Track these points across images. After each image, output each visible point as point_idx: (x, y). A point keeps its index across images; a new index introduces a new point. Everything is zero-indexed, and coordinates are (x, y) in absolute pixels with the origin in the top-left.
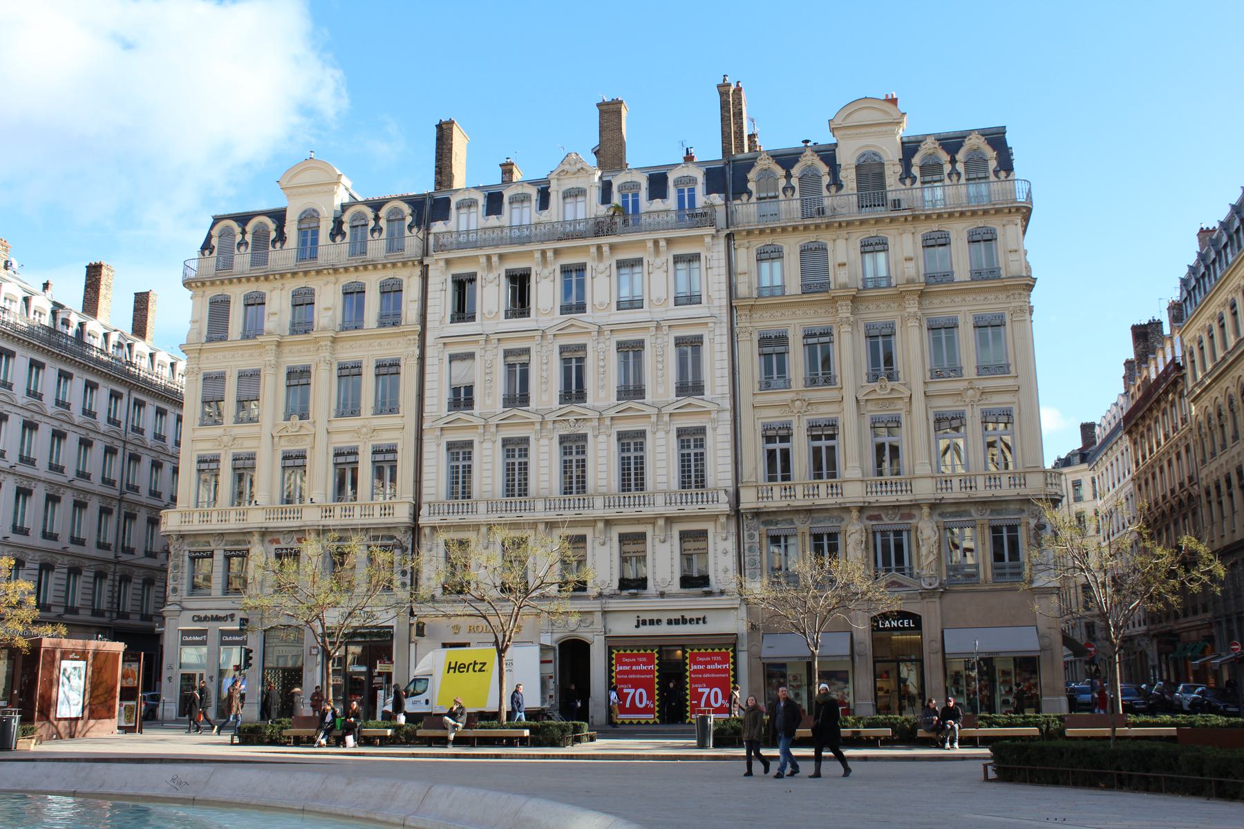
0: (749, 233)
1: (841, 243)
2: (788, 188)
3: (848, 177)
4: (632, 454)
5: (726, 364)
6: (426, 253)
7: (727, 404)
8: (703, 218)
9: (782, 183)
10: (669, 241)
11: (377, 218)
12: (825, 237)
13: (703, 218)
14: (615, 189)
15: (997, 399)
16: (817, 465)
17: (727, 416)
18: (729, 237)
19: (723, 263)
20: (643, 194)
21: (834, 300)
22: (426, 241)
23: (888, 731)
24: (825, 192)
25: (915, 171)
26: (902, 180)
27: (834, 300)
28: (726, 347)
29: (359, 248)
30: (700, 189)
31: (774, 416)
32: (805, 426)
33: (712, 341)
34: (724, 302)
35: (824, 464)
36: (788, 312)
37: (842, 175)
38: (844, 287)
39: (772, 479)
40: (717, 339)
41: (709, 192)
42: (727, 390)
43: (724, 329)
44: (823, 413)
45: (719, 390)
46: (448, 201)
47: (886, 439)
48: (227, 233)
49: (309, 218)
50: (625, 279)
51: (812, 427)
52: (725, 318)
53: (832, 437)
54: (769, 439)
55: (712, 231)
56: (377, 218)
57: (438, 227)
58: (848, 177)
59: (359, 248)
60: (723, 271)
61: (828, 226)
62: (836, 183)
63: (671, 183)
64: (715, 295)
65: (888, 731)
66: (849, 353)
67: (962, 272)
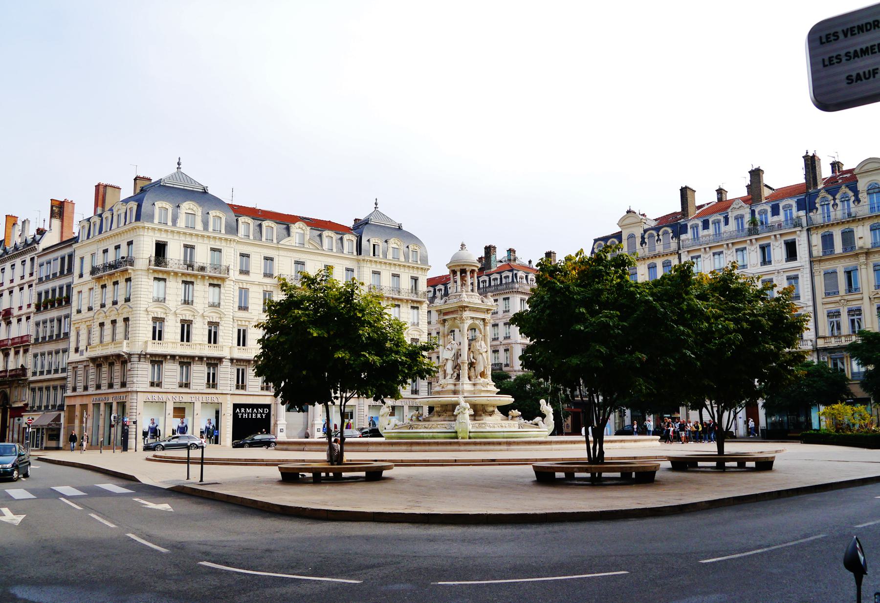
0: (817, 228)
1: (860, 228)
5: (810, 286)
6: (679, 249)
7: (811, 303)
8: (797, 224)
10: (733, 244)
11: (658, 235)
12: (853, 226)
13: (797, 224)
14: (756, 213)
18: (808, 230)
19: (806, 242)
20: (769, 214)
21: (857, 255)
22: (679, 243)
23: (363, 474)
27: (857, 255)
28: (809, 279)
29: (652, 248)
30: (794, 209)
31: (832, 307)
32: (846, 310)
33: (802, 276)
34: (807, 259)
36: (837, 261)
37: (860, 196)
38: (861, 248)
41: (798, 210)
42: (810, 297)
43: (808, 270)
44: (854, 305)
45: (807, 298)
46: (686, 225)
48: (600, 245)
49: (631, 237)
50: (717, 261)
51: (849, 311)
52: (808, 266)
55: (800, 229)
56: (658, 235)
57: (683, 237)
59: (652, 248)
60: (806, 245)
61: (853, 221)
62: (857, 200)
63: (781, 208)
64: (803, 256)
65: (363, 474)
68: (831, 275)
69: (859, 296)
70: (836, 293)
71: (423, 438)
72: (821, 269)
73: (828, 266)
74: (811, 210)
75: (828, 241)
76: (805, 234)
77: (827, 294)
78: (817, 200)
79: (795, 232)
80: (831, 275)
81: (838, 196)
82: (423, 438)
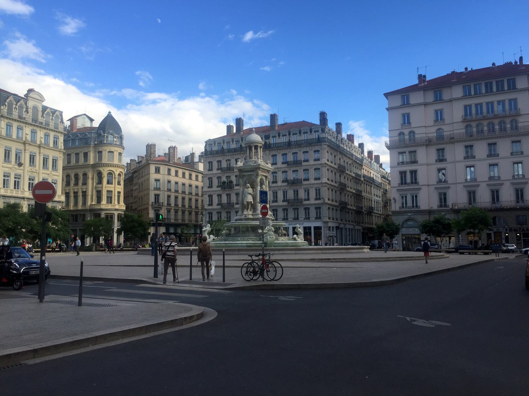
1: (27, 128)
3: (30, 111)
16: (15, 185)
26: (42, 117)
35: (17, 185)
36: (12, 143)
37: (29, 110)
39: (15, 188)
47: (31, 182)
54: (4, 176)
62: (27, 111)
78: (8, 101)
81: (18, 104)
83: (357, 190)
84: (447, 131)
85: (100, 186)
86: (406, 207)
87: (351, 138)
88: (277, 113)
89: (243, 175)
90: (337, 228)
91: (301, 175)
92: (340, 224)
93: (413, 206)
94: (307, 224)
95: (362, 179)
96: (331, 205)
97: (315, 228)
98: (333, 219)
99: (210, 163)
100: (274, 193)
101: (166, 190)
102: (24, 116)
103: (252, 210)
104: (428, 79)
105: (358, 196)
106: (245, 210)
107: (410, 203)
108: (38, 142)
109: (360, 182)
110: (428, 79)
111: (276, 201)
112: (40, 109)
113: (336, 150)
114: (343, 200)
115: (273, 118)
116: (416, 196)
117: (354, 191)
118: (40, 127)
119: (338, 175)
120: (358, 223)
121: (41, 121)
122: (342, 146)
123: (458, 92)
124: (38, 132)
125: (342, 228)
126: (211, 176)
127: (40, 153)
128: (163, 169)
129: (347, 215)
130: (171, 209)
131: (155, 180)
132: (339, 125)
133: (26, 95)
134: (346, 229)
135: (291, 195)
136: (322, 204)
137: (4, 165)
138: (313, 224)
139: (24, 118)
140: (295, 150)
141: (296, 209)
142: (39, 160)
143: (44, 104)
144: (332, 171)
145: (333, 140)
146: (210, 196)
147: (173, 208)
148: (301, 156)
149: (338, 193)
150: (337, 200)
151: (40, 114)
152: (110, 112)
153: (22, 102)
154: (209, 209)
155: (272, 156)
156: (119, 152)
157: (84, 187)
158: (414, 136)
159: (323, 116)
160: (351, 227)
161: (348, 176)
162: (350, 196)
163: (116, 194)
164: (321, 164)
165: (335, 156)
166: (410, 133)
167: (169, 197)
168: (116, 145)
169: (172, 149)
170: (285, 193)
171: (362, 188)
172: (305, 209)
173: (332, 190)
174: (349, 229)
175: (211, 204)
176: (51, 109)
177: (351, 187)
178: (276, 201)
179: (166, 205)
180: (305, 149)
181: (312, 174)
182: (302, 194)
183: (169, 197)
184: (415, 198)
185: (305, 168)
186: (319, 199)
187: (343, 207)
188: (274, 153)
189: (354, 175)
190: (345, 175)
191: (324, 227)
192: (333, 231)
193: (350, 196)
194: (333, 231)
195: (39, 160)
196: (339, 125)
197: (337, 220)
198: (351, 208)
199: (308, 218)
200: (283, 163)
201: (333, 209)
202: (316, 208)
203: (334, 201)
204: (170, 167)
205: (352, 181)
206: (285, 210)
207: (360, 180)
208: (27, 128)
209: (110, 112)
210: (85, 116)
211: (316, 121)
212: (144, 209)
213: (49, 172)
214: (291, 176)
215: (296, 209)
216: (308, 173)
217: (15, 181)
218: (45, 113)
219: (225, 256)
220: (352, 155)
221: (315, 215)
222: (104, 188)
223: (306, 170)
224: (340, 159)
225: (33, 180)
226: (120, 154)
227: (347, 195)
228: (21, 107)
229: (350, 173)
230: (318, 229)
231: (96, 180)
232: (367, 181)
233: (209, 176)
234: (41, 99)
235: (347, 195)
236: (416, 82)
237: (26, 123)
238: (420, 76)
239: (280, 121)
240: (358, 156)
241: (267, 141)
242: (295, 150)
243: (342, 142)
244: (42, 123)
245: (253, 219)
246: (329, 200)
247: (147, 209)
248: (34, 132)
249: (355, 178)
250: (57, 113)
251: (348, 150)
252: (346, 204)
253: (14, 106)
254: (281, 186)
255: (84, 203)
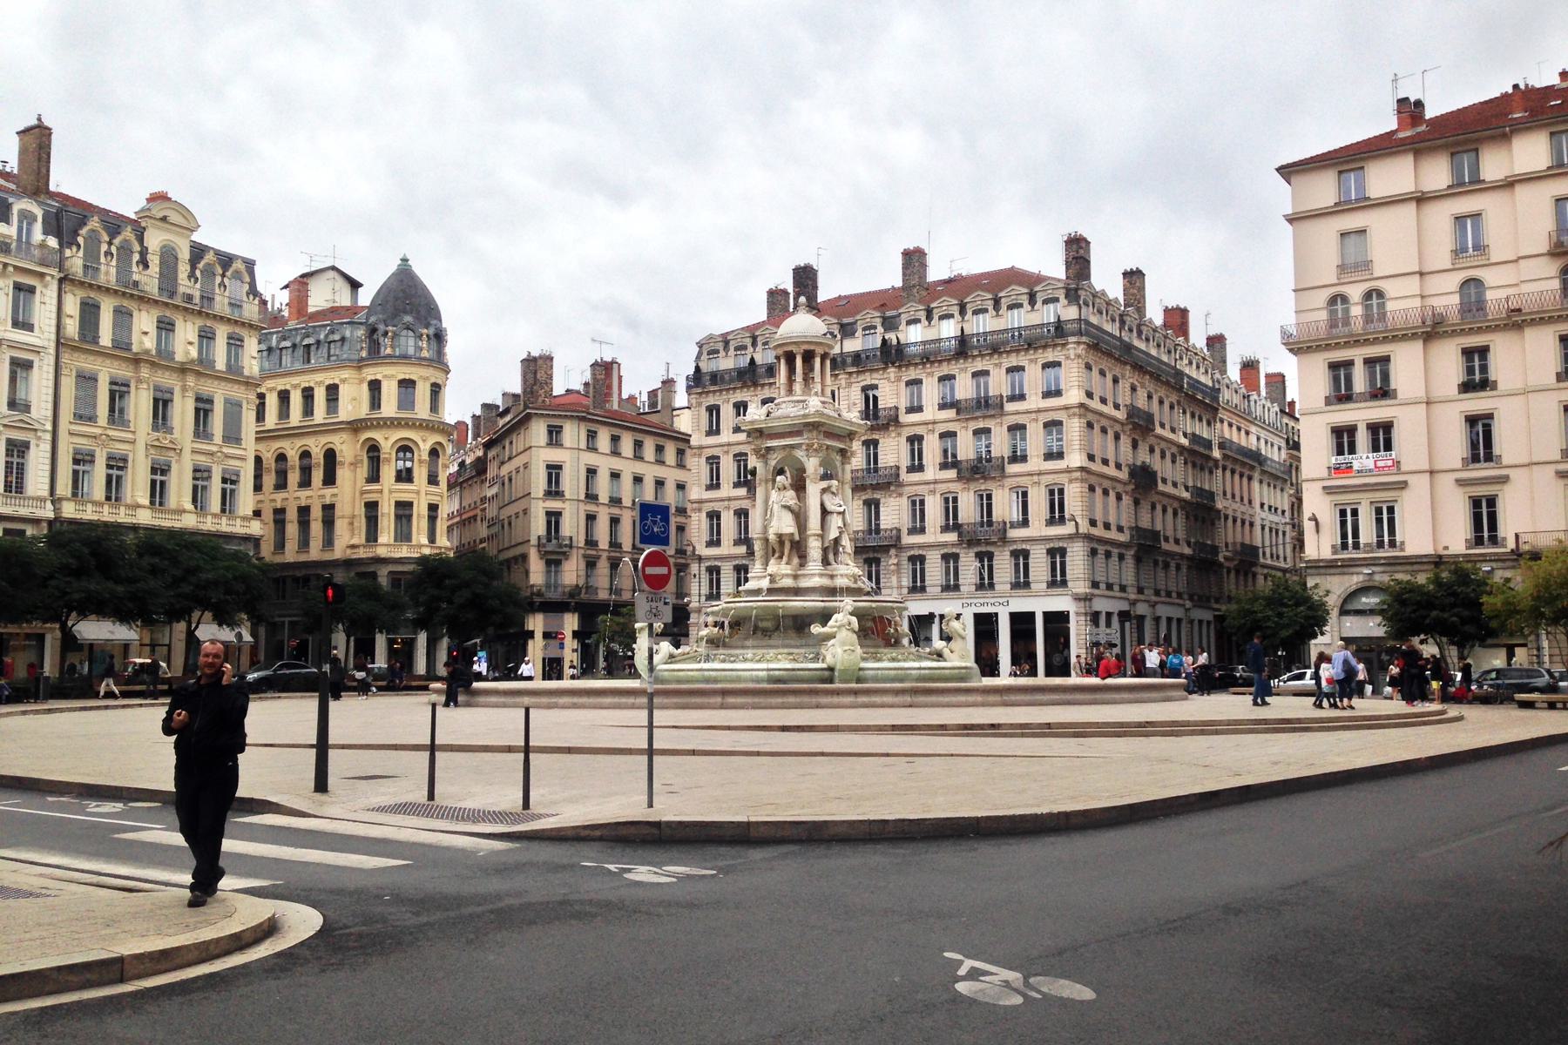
2: (108, 253)
3: (154, 261)
4: (15, 460)
7: (49, 427)
9: (104, 247)
15: (232, 462)
17: (48, 437)
18: (61, 281)
19: (55, 301)
24: (135, 268)
25: (198, 273)
26: (189, 277)
28: (51, 376)
30: (38, 227)
33: (40, 367)
34: (53, 337)
36: (100, 360)
40: (45, 368)
42: (50, 413)
44: (120, 448)
45: (43, 412)
52: (52, 351)
53: (119, 468)
58: (154, 261)
62: (144, 263)
64: (46, 328)
66: (140, 405)
67: (221, 364)
68: (87, 380)
69: (130, 436)
70: (92, 419)
71: (716, 681)
72: (75, 362)
73: (88, 364)
74: (70, 245)
75: (89, 312)
76: (54, 286)
77: (79, 417)
78: (84, 231)
79: (42, 275)
80: (87, 380)
81: (117, 241)
82: (688, 681)
83: (1199, 492)
84: (1500, 286)
85: (375, 487)
86: (1356, 546)
87: (1178, 319)
88: (924, 246)
89: (769, 449)
90: (1124, 616)
91: (1000, 444)
92: (1133, 603)
93: (1380, 544)
94: (1021, 604)
95: (1216, 454)
96: (1100, 540)
97: (1048, 616)
98: (1109, 587)
99: (714, 410)
100: (914, 503)
101: (582, 497)
102: (136, 277)
103: (796, 561)
104: (1430, 113)
105: (1202, 511)
106: (772, 561)
107: (1367, 534)
108: (179, 357)
109: (1211, 464)
110: (1430, 113)
111: (922, 530)
112: (184, 254)
113: (1117, 360)
114: (1145, 523)
115: (914, 259)
116: (1391, 510)
117: (1186, 495)
118: (186, 309)
119: (1125, 442)
120: (1201, 601)
121: (189, 291)
122: (1142, 345)
123: (1531, 152)
124: (180, 325)
125: (1141, 618)
126: (715, 452)
127: (184, 389)
128: (573, 433)
129: (1161, 574)
130: (599, 557)
131: (548, 467)
132: (1134, 277)
133: (144, 213)
134: (1157, 619)
135: (968, 510)
136: (1071, 537)
137: (74, 427)
138: (1039, 603)
139: (136, 284)
140: (979, 365)
141: (985, 558)
142: (182, 412)
143: (197, 237)
144: (1104, 431)
145: (1108, 327)
146: (714, 516)
147: (605, 555)
148: (999, 383)
149: (1126, 500)
150: (1123, 524)
151: (183, 269)
152: (405, 260)
153: (128, 234)
154: (708, 558)
155: (909, 383)
156: (433, 380)
157: (328, 492)
158: (1382, 306)
159: (1077, 251)
160: (1176, 613)
161: (1163, 445)
162: (1170, 511)
163: (425, 511)
164: (1066, 408)
165: (1116, 381)
166: (1368, 295)
167: (591, 518)
168: (422, 362)
169: (605, 371)
170: (951, 505)
171: (1217, 482)
172: (1015, 554)
173: (1106, 492)
174: (1169, 620)
175: (714, 542)
176: (218, 253)
177: (1175, 478)
178: (922, 530)
179: (582, 544)
180: (1013, 360)
181: (1036, 441)
182: (1005, 507)
183: (591, 518)
184: (1386, 517)
185: (1012, 420)
186: (1062, 520)
187: (1146, 547)
188: (913, 373)
189: (1185, 442)
190: (1152, 440)
191: (1077, 614)
192: (1108, 625)
193: (1170, 511)
194: (1108, 625)
195: (182, 412)
196: (1134, 277)
197: (1123, 588)
198: (1176, 549)
199: (1022, 584)
200: (943, 406)
201: (1108, 555)
202: (1051, 552)
203: (1113, 527)
204: (593, 427)
205: (1180, 460)
206: (950, 558)
207: (1209, 458)
208: (144, 313)
209: (405, 260)
210: (332, 274)
211: (1055, 267)
212: (515, 559)
213: (215, 449)
214: (966, 448)
215: (985, 558)
216: (1023, 439)
217: (109, 477)
218: (201, 266)
219: (656, 712)
220: (1180, 374)
221: (975, 579)
222: (386, 491)
223: (1017, 429)
224: (1133, 389)
225: (164, 472)
226: (436, 389)
227: (1159, 508)
228: (125, 250)
229: (1171, 436)
230: (1057, 621)
231: (363, 471)
232: (1235, 460)
233: (710, 452)
234: (189, 224)
235: (1159, 508)
236: (1387, 122)
237: (141, 299)
238: (1402, 102)
239: (936, 272)
240: (1203, 379)
241: (892, 336)
242: (979, 365)
243: (1140, 333)
244: (189, 298)
245: (797, 591)
246: (1093, 523)
247: (524, 558)
248: (165, 327)
249: (1191, 452)
250: (238, 265)
251: (1165, 358)
252: (1155, 535)
253: (104, 247)
254: (936, 482)
255: (329, 542)
